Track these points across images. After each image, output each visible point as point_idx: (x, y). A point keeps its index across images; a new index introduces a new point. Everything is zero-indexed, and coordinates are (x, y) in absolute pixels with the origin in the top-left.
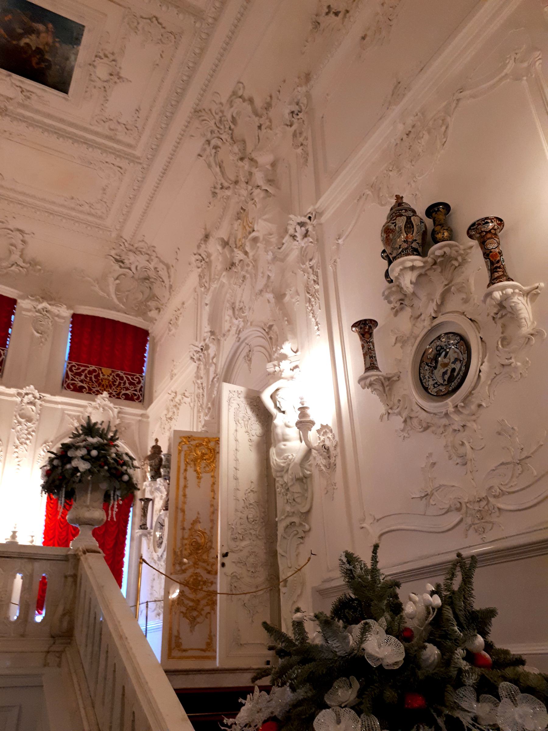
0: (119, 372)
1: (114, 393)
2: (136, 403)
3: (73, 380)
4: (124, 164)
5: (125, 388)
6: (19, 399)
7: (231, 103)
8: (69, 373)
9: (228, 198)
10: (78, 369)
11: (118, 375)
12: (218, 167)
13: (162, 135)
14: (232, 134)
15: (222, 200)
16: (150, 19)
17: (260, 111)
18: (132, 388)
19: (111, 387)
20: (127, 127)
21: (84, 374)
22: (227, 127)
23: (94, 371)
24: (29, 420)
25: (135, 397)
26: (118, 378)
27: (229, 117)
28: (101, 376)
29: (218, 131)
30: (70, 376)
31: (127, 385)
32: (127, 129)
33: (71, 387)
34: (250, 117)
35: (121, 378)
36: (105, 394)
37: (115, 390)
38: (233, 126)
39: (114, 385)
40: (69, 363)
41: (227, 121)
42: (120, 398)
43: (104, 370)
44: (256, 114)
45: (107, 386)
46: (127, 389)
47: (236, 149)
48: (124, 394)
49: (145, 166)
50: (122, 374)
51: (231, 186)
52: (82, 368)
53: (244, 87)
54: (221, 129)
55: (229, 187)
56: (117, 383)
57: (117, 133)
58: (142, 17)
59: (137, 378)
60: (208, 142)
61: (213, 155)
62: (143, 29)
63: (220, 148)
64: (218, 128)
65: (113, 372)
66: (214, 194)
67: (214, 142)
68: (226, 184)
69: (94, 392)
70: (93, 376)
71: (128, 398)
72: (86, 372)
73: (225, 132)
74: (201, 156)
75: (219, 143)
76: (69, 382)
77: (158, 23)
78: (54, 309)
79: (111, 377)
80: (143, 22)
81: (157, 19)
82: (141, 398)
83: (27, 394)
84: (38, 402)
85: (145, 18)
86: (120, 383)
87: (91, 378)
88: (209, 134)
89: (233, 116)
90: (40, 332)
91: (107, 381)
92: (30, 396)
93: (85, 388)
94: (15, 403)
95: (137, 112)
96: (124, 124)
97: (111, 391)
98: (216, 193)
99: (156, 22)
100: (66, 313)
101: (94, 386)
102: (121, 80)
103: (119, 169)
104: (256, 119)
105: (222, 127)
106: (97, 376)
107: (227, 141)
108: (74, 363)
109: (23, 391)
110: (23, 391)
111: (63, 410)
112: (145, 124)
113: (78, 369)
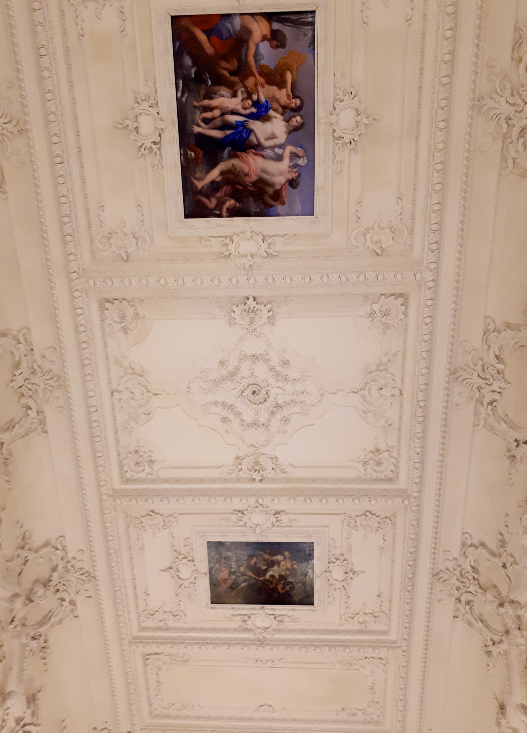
4: (382, 653)
7: (465, 555)
9: (506, 653)
12: (480, 622)
13: (411, 611)
14: (479, 584)
15: (499, 656)
16: (364, 514)
17: (496, 550)
20: (374, 615)
22: (471, 578)
27: (470, 569)
29: (464, 586)
32: (376, 617)
34: (489, 560)
38: (476, 576)
41: (468, 572)
44: (494, 555)
47: (490, 596)
49: (405, 648)
51: (503, 638)
53: (470, 535)
54: (466, 582)
55: (502, 640)
57: (367, 624)
58: (357, 516)
60: (459, 600)
61: (469, 612)
62: (361, 524)
63: (472, 601)
64: (462, 582)
66: (489, 653)
67: (464, 598)
68: (496, 638)
73: (471, 584)
74: (457, 617)
75: (470, 597)
77: (373, 515)
80: (358, 520)
81: (370, 512)
85: (361, 515)
88: (456, 592)
89: (472, 566)
95: (379, 597)
96: (372, 614)
98: (490, 652)
99: (370, 515)
102: (356, 574)
103: (380, 660)
104: (496, 560)
105: (466, 580)
107: (476, 592)
112: (390, 606)
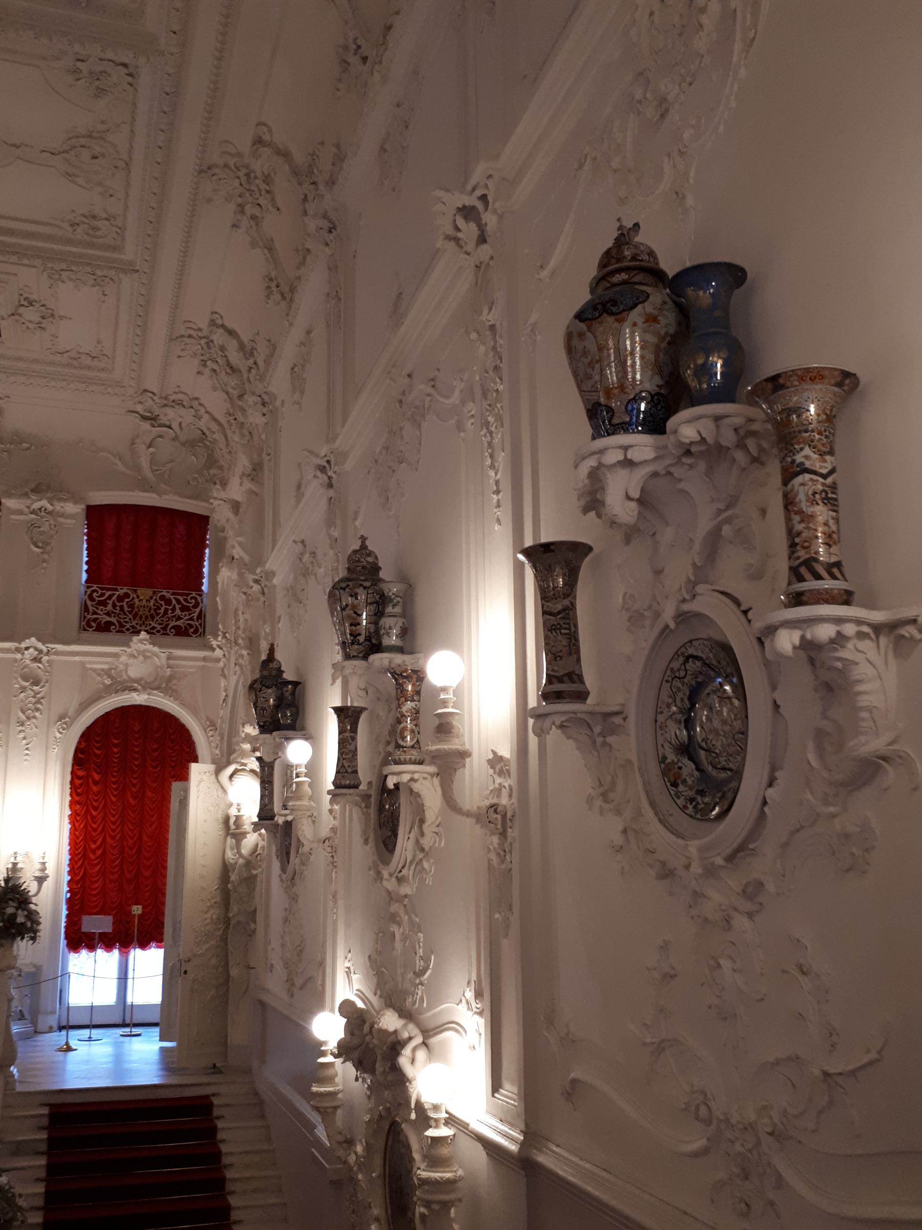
0: (164, 593)
1: (159, 627)
2: (194, 640)
3: (95, 613)
5: (174, 616)
6: (19, 656)
8: (89, 603)
10: (102, 595)
11: (162, 598)
18: (185, 616)
19: (152, 617)
21: (111, 602)
23: (127, 595)
24: (36, 683)
25: (192, 630)
26: (163, 603)
28: (136, 601)
30: (91, 608)
31: (178, 612)
33: (93, 624)
35: (168, 602)
36: (143, 635)
37: (159, 621)
39: (158, 614)
40: (88, 587)
42: (167, 634)
43: (140, 591)
45: (147, 617)
46: (179, 618)
48: (172, 627)
50: (168, 595)
52: (109, 593)
56: (162, 611)
59: (192, 598)
65: (154, 593)
69: (128, 630)
70: (124, 604)
71: (181, 632)
72: (114, 598)
76: (89, 616)
78: (58, 506)
79: (152, 602)
82: (201, 630)
83: (27, 649)
84: (45, 658)
86: (166, 610)
87: (122, 607)
90: (40, 545)
91: (147, 610)
92: (31, 650)
93: (114, 624)
94: (16, 660)
97: (153, 624)
100: (75, 509)
101: (127, 620)
106: (131, 606)
108: (95, 587)
109: (23, 645)
110: (23, 645)
111: (82, 664)
113: (102, 595)
